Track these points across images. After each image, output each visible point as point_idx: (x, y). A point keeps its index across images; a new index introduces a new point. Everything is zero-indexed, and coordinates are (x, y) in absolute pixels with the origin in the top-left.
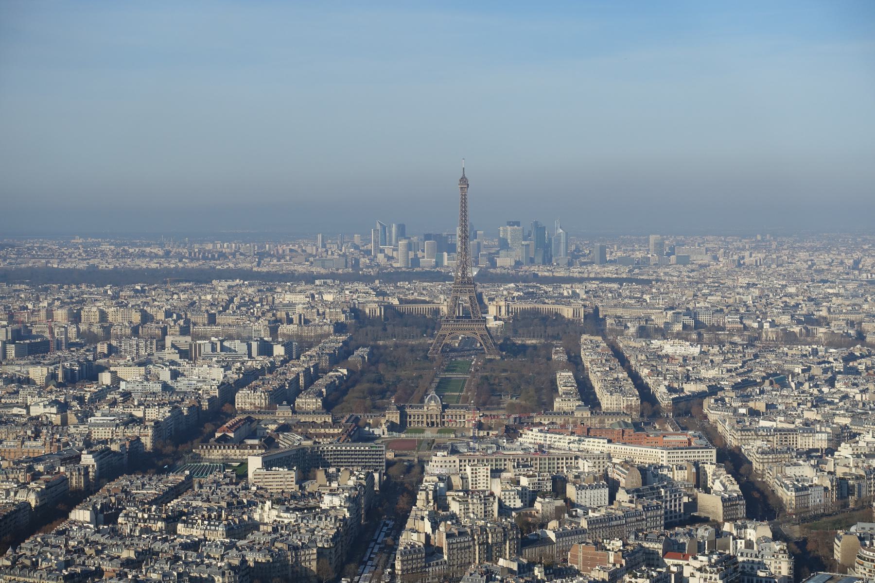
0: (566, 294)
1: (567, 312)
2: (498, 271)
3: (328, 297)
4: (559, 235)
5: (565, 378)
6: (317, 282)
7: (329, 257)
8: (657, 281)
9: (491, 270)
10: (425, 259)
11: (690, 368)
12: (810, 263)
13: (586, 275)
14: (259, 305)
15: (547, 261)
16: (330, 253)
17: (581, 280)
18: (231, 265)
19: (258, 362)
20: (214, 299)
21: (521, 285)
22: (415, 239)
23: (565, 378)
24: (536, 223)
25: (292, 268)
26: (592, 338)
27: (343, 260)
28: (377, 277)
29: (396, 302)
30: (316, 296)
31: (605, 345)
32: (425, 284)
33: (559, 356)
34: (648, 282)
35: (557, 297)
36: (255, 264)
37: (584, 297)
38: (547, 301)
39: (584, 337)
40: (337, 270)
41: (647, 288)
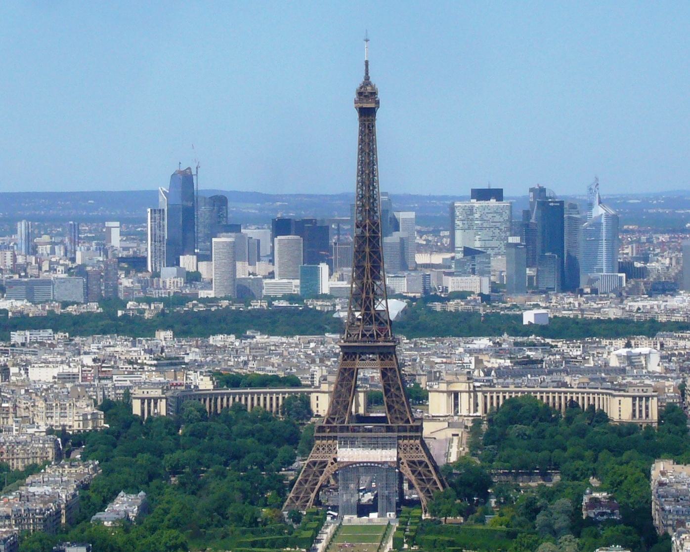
0: (614, 363)
1: (620, 410)
3: (42, 374)
4: (597, 224)
6: (17, 337)
7: (44, 276)
10: (277, 280)
13: (663, 319)
15: (569, 283)
16: (45, 266)
17: (650, 328)
21: (507, 340)
22: (251, 232)
24: (542, 190)
26: (678, 468)
27: (81, 281)
29: (205, 384)
30: (13, 370)
32: (275, 339)
38: (568, 379)
40: (65, 305)
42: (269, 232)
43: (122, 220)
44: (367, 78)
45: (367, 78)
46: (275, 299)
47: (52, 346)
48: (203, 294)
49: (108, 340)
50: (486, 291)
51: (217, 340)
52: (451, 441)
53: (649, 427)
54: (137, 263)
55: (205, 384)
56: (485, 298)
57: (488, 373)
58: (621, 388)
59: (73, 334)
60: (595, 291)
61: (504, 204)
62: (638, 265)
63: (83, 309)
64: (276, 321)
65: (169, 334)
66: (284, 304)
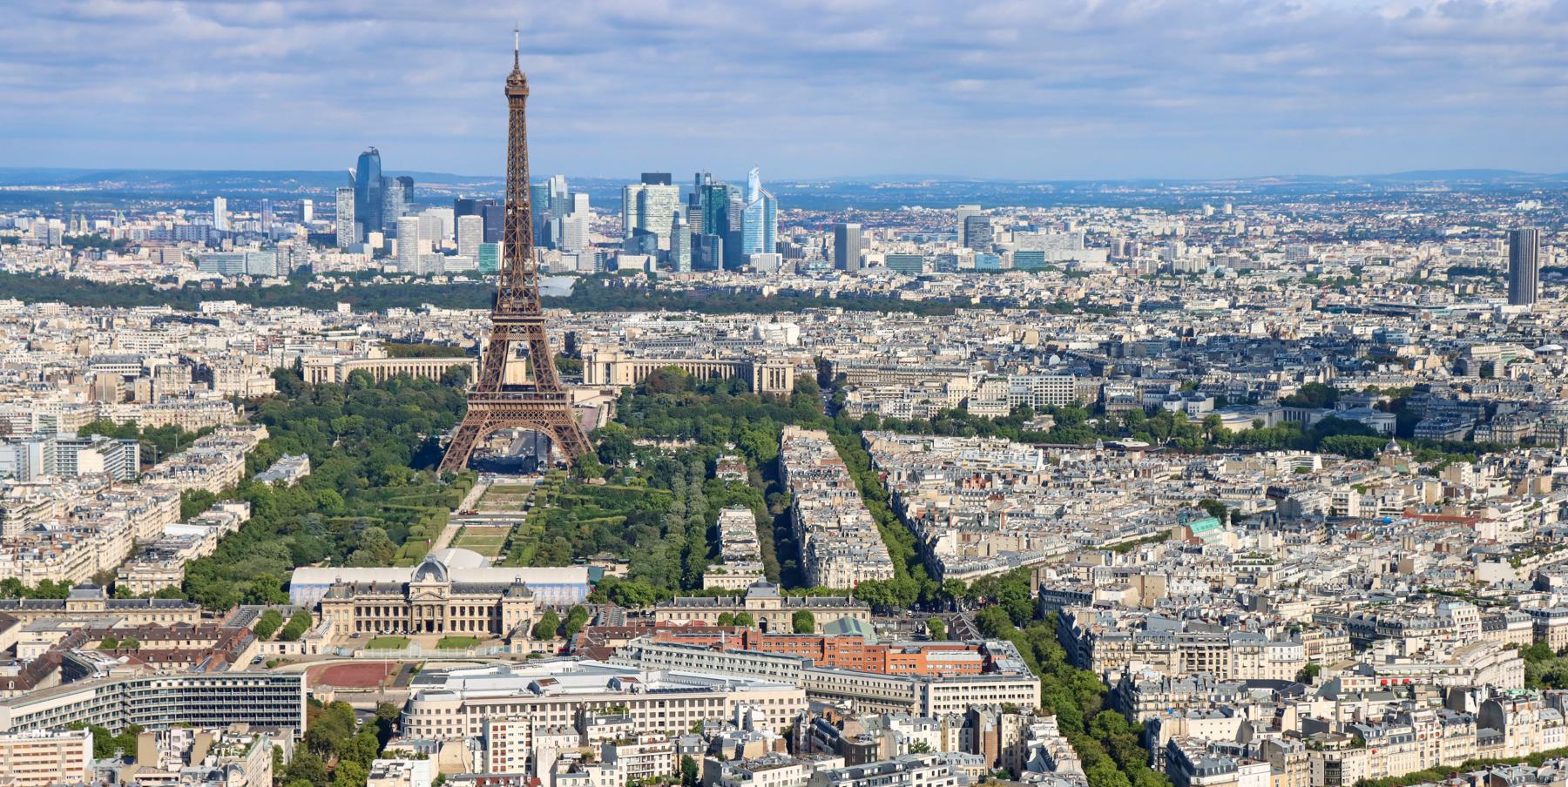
3: (215, 343)
5: (738, 522)
12: (1310, 268)
23: (738, 522)
26: (805, 433)
31: (831, 449)
32: (446, 312)
42: (451, 212)
43: (316, 199)
44: (517, 67)
45: (517, 67)
46: (456, 274)
48: (388, 269)
49: (287, 311)
51: (393, 313)
52: (601, 408)
54: (325, 241)
58: (764, 359)
59: (256, 306)
62: (794, 245)
63: (272, 282)
64: (450, 296)
66: (464, 279)
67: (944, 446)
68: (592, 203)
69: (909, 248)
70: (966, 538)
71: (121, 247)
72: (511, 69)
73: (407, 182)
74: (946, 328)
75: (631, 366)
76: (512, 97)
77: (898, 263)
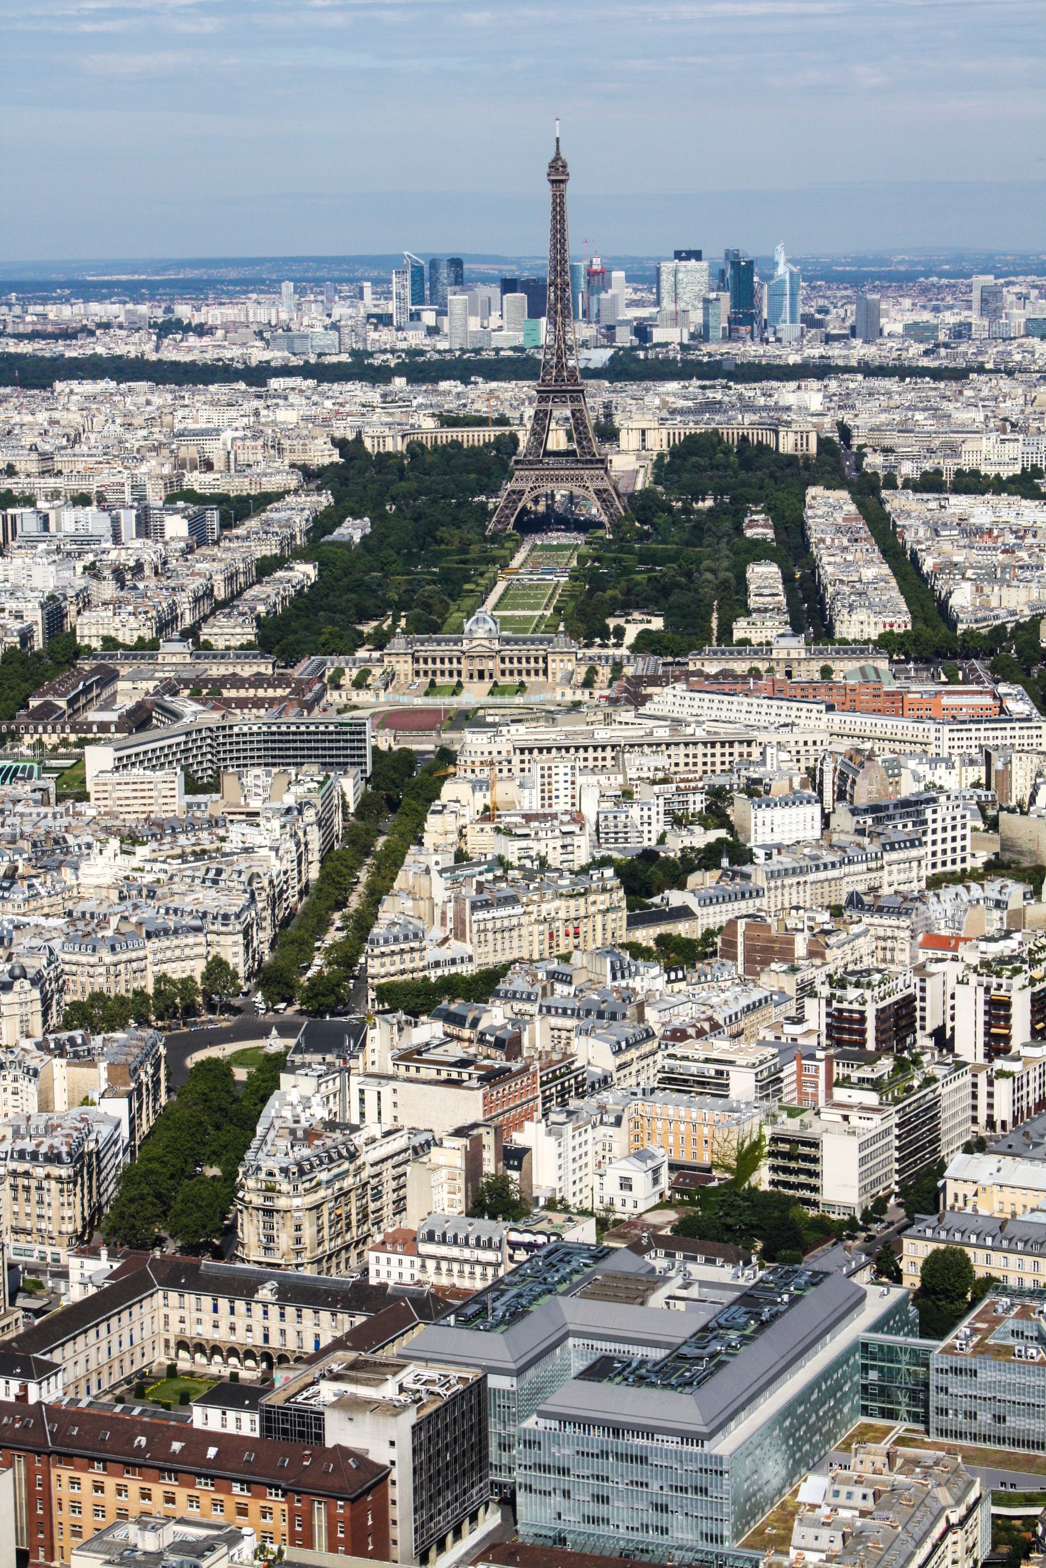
2: (651, 355)
3: (287, 416)
5: (764, 577)
8: (981, 370)
9: (641, 355)
11: (1023, 554)
14: (144, 433)
18: (100, 350)
19: (137, 549)
20: (53, 422)
23: (764, 577)
25: (228, 354)
26: (828, 493)
28: (400, 370)
30: (263, 412)
31: (852, 508)
32: (494, 385)
33: (759, 528)
34: (959, 375)
35: (766, 408)
36: (151, 345)
37: (820, 408)
39: (812, 491)
40: (320, 355)
41: (954, 385)
43: (375, 282)
44: (558, 153)
45: (558, 153)
47: (301, 391)
49: (349, 386)
50: (686, 341)
51: (444, 385)
53: (806, 458)
54: (383, 320)
55: (429, 423)
56: (684, 347)
57: (673, 412)
58: (788, 424)
59: (320, 381)
60: (779, 340)
61: (704, 264)
62: (818, 316)
63: (334, 359)
65: (404, 380)
66: (510, 353)
67: (959, 504)
68: (629, 279)
69: (926, 316)
70: (979, 590)
71: (202, 330)
72: (552, 155)
73: (456, 263)
74: (961, 392)
75: (665, 432)
76: (553, 182)
77: (916, 332)
